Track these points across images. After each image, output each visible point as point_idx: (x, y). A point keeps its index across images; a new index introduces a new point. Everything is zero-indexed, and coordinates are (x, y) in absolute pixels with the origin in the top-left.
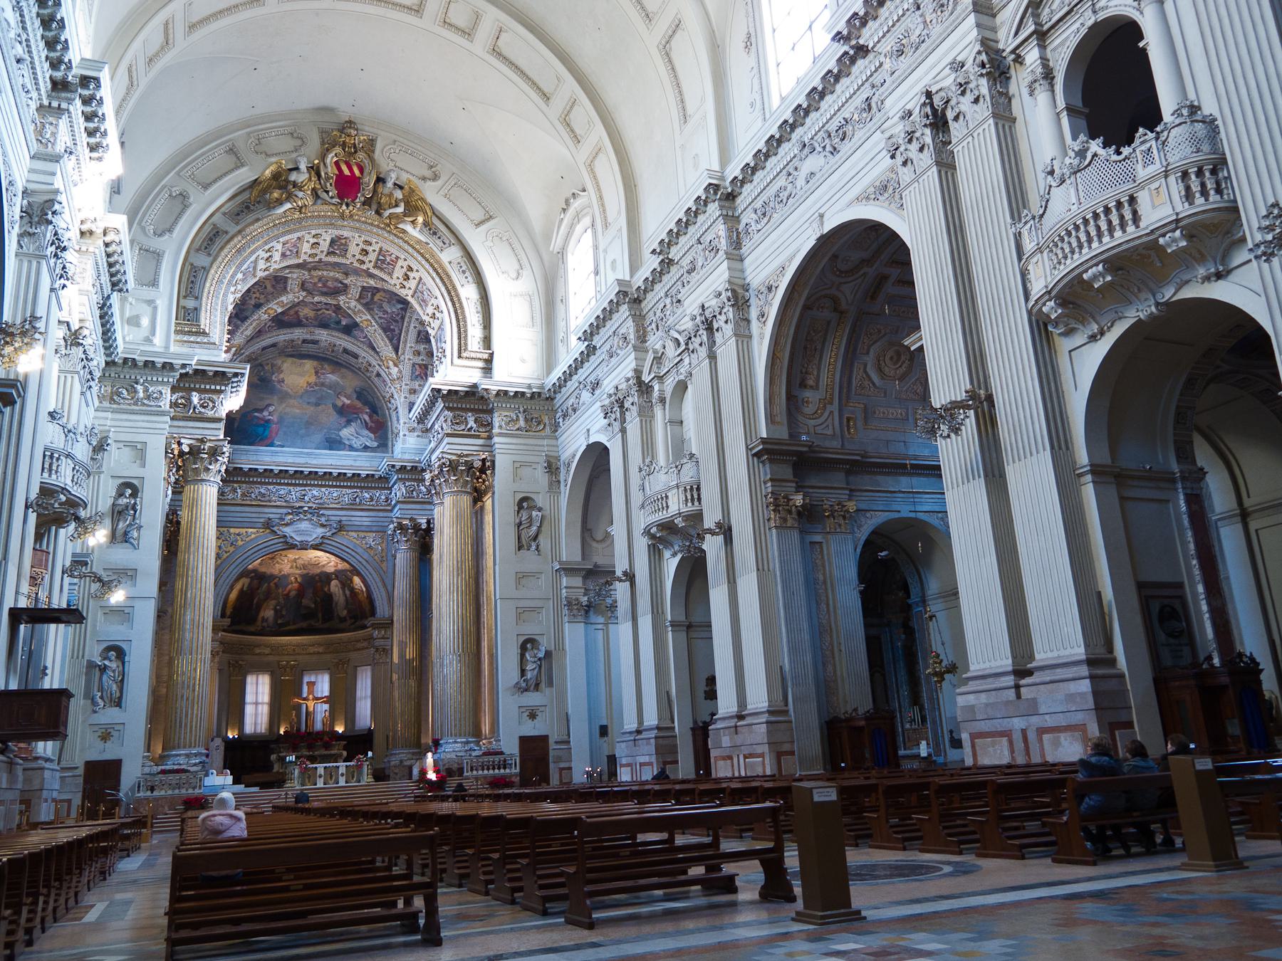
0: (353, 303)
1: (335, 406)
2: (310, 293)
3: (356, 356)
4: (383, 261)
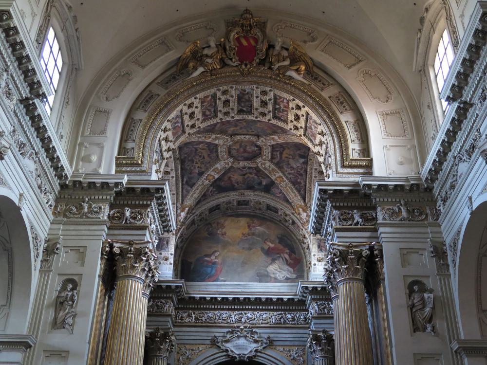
0: (268, 164)
1: (262, 249)
2: (236, 159)
3: (276, 210)
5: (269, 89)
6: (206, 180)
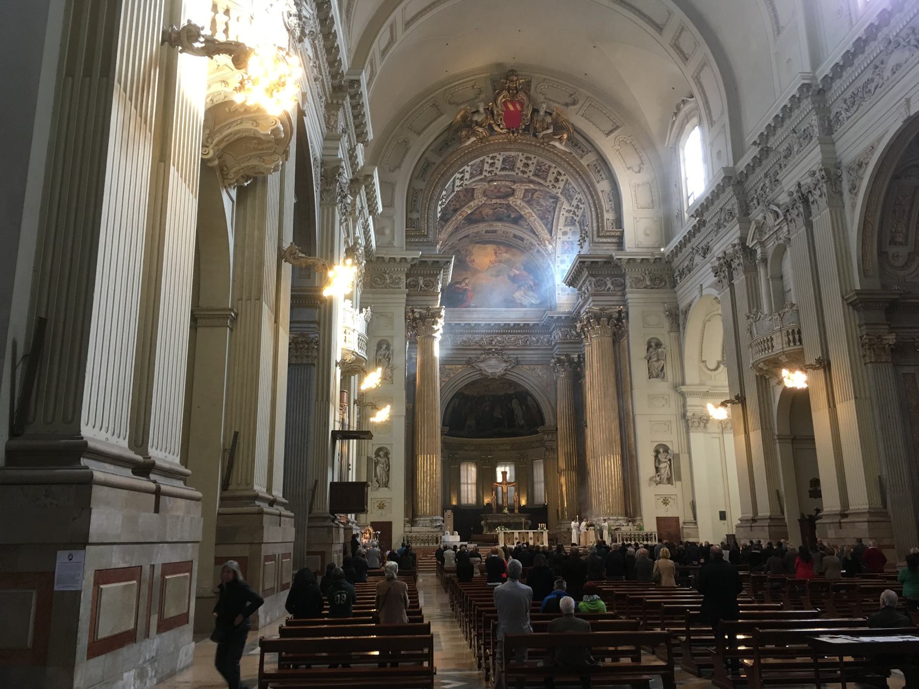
0: (519, 202)
1: (509, 276)
3: (522, 239)
4: (540, 170)
6: (460, 215)
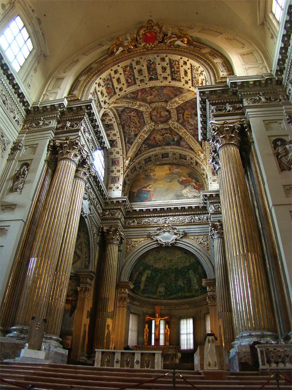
0: (176, 124)
1: (178, 181)
5: (165, 55)
6: (140, 139)
